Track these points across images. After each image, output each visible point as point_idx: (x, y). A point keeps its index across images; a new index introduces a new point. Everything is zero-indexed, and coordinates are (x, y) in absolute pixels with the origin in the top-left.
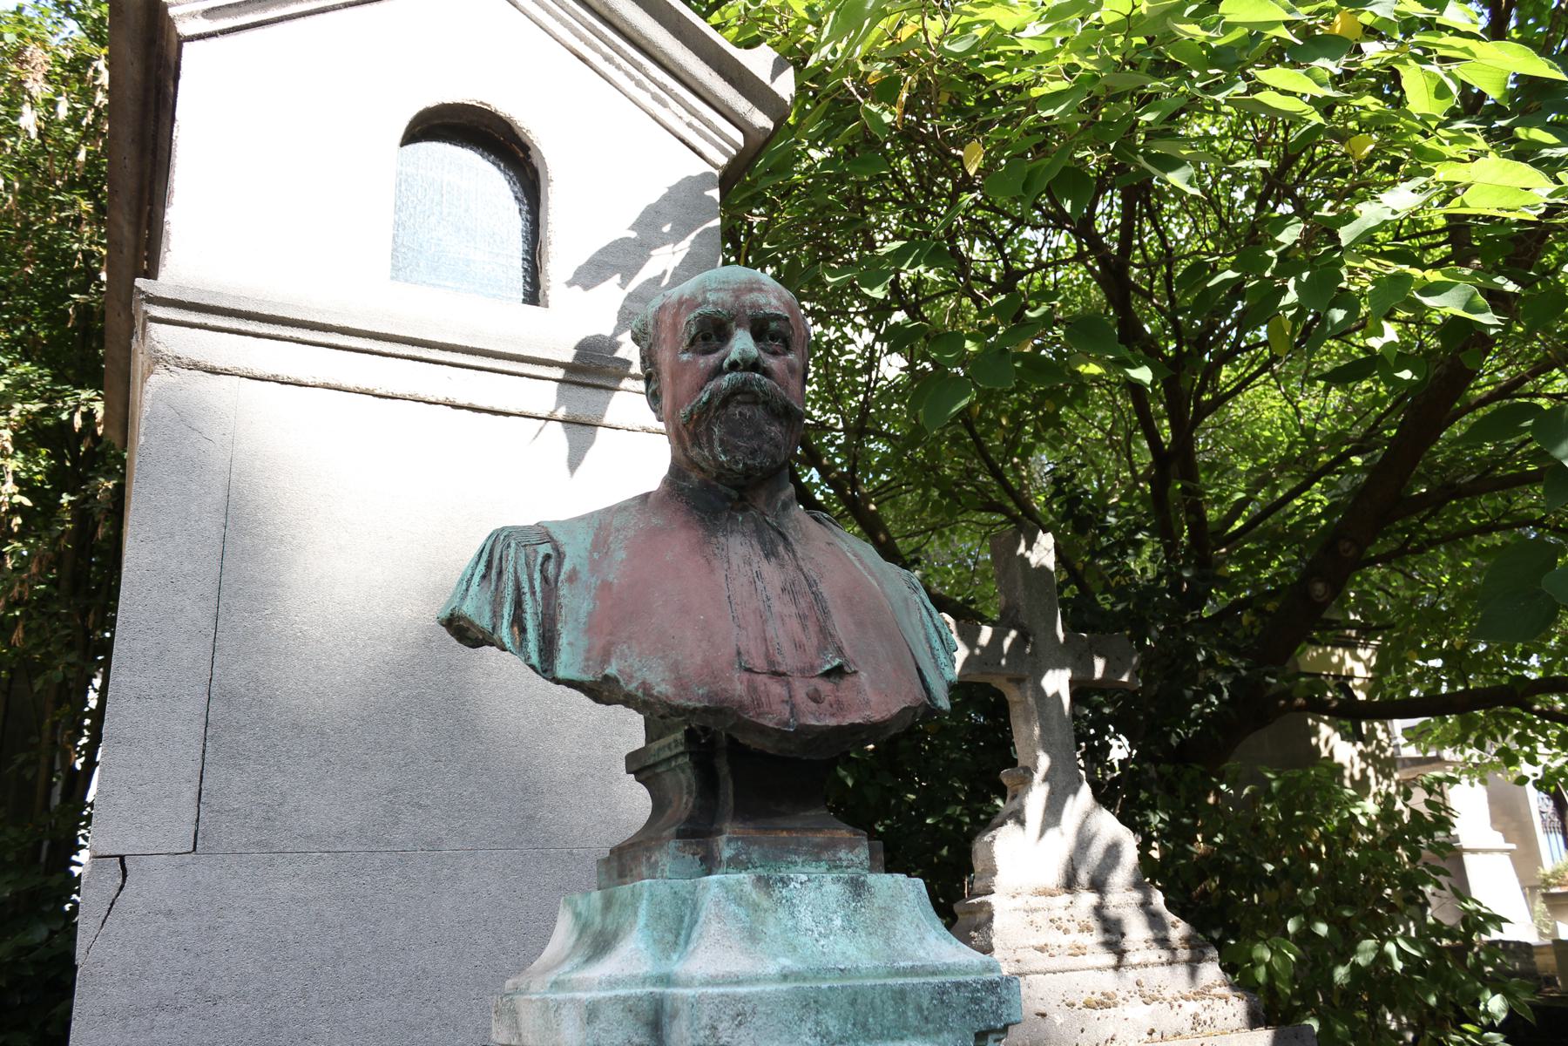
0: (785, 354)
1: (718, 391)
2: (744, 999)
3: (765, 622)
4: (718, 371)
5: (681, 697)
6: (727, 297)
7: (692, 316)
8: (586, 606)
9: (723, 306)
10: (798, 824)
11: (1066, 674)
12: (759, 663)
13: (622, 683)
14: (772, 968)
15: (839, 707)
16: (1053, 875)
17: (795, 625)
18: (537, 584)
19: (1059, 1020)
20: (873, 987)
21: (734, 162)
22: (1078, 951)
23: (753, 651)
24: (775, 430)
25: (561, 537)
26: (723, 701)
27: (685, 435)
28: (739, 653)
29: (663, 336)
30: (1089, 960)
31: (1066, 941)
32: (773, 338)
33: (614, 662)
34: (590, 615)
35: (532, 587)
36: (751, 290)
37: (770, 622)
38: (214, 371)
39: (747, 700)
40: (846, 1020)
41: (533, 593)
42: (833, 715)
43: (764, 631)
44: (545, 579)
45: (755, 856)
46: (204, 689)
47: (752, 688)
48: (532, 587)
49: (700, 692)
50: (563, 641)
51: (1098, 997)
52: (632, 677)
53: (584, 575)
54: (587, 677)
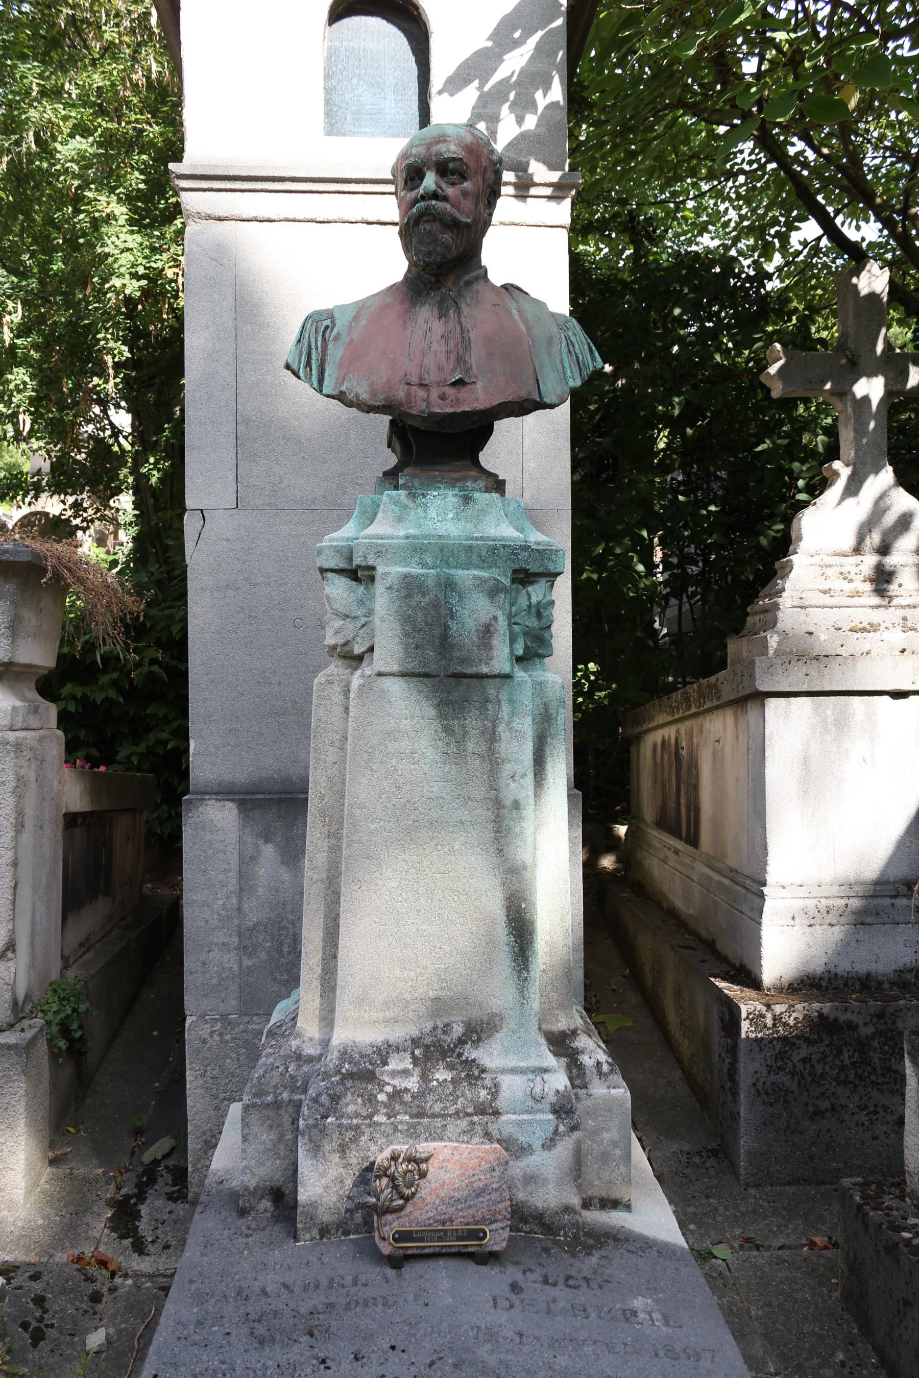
0: (461, 183)
1: (412, 215)
2: (382, 545)
4: (416, 201)
6: (422, 150)
8: (340, 354)
10: (447, 468)
12: (415, 380)
14: (402, 533)
15: (458, 401)
16: (849, 542)
17: (442, 357)
18: (319, 345)
19: (823, 637)
20: (454, 544)
22: (858, 594)
23: (413, 373)
24: (447, 237)
31: (848, 587)
32: (452, 174)
34: (341, 358)
36: (438, 142)
38: (220, 219)
40: (437, 559)
41: (317, 348)
42: (452, 407)
45: (416, 484)
46: (232, 418)
47: (408, 394)
50: (327, 374)
51: (865, 625)
54: (335, 393)
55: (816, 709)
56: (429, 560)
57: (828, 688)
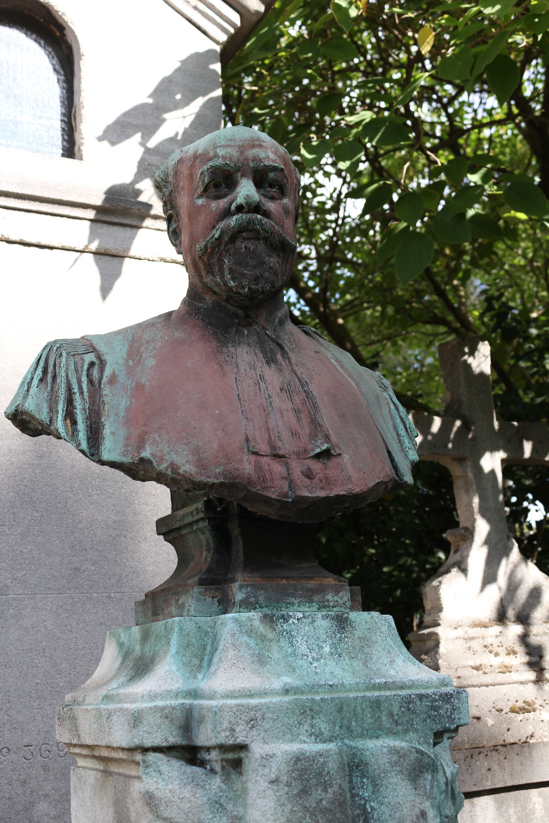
0: (281, 199)
1: (228, 227)
2: (255, 708)
3: (267, 415)
4: (227, 213)
5: (202, 475)
6: (234, 153)
7: (205, 168)
8: (124, 404)
9: (230, 160)
10: (295, 574)
12: (264, 448)
13: (155, 464)
14: (277, 684)
19: (490, 722)
20: (355, 699)
21: (232, 38)
22: (506, 669)
23: (258, 438)
25: (102, 348)
26: (235, 478)
27: (201, 265)
28: (247, 440)
29: (181, 184)
30: (514, 676)
31: (496, 661)
32: (271, 186)
33: (147, 447)
34: (127, 410)
35: (80, 388)
36: (253, 146)
37: (272, 416)
39: (254, 478)
40: (334, 724)
41: (82, 393)
42: (322, 488)
43: (267, 422)
44: (91, 382)
45: (261, 599)
47: (259, 468)
48: (80, 388)
49: (217, 471)
50: (107, 431)
51: (520, 704)
52: (162, 459)
53: (122, 377)
54: (126, 460)
55: (499, 807)
56: (323, 726)
57: (510, 784)
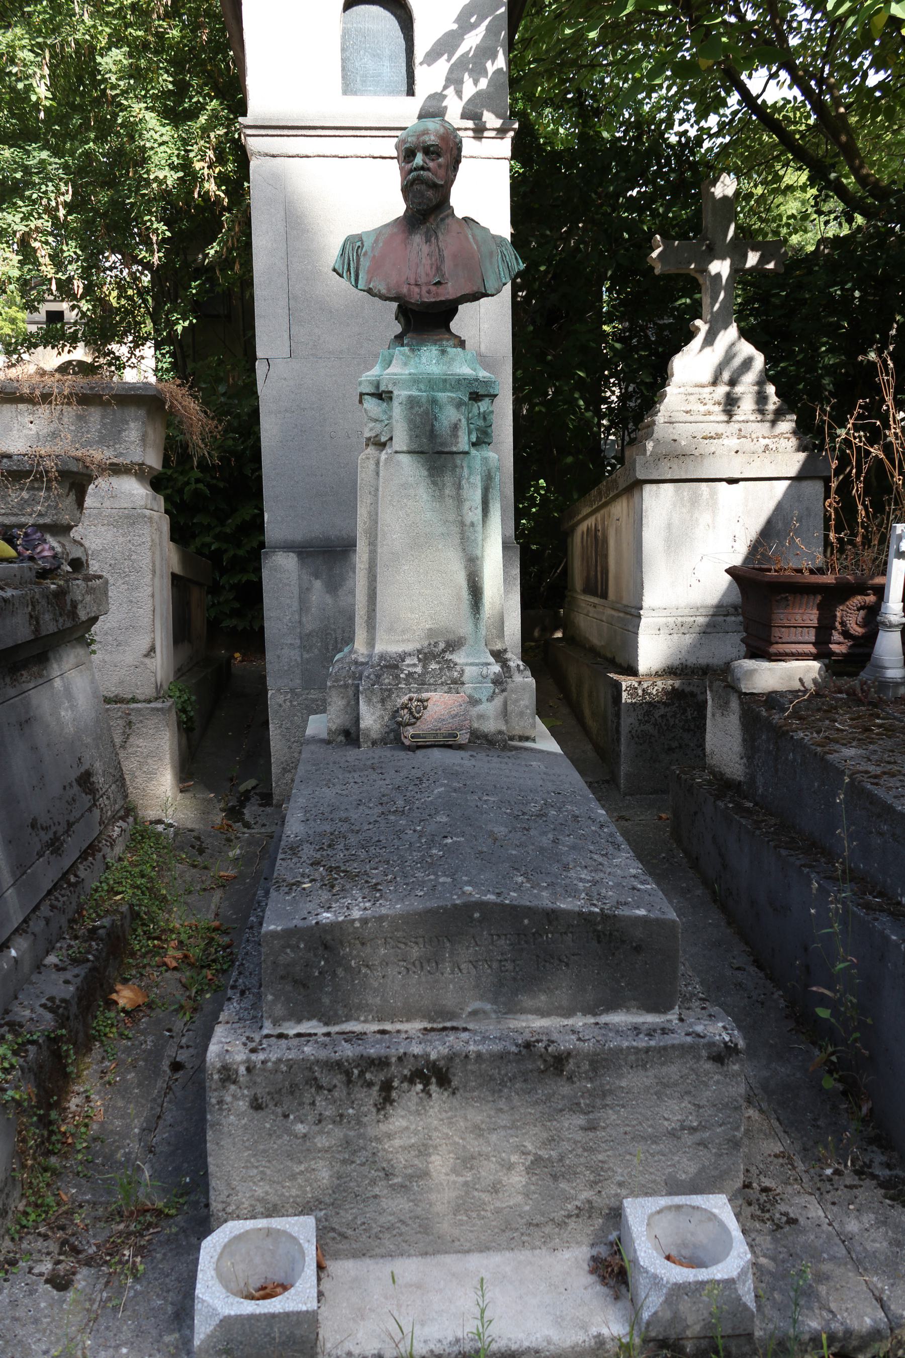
4: (411, 171)
6: (414, 139)
11: (727, 263)
12: (413, 282)
14: (407, 372)
15: (437, 294)
16: (708, 377)
17: (428, 268)
19: (683, 443)
22: (709, 413)
24: (430, 193)
30: (712, 418)
31: (703, 408)
38: (273, 156)
46: (285, 296)
47: (409, 290)
51: (713, 434)
53: (369, 253)
55: (676, 491)
56: (422, 387)
57: (684, 477)
